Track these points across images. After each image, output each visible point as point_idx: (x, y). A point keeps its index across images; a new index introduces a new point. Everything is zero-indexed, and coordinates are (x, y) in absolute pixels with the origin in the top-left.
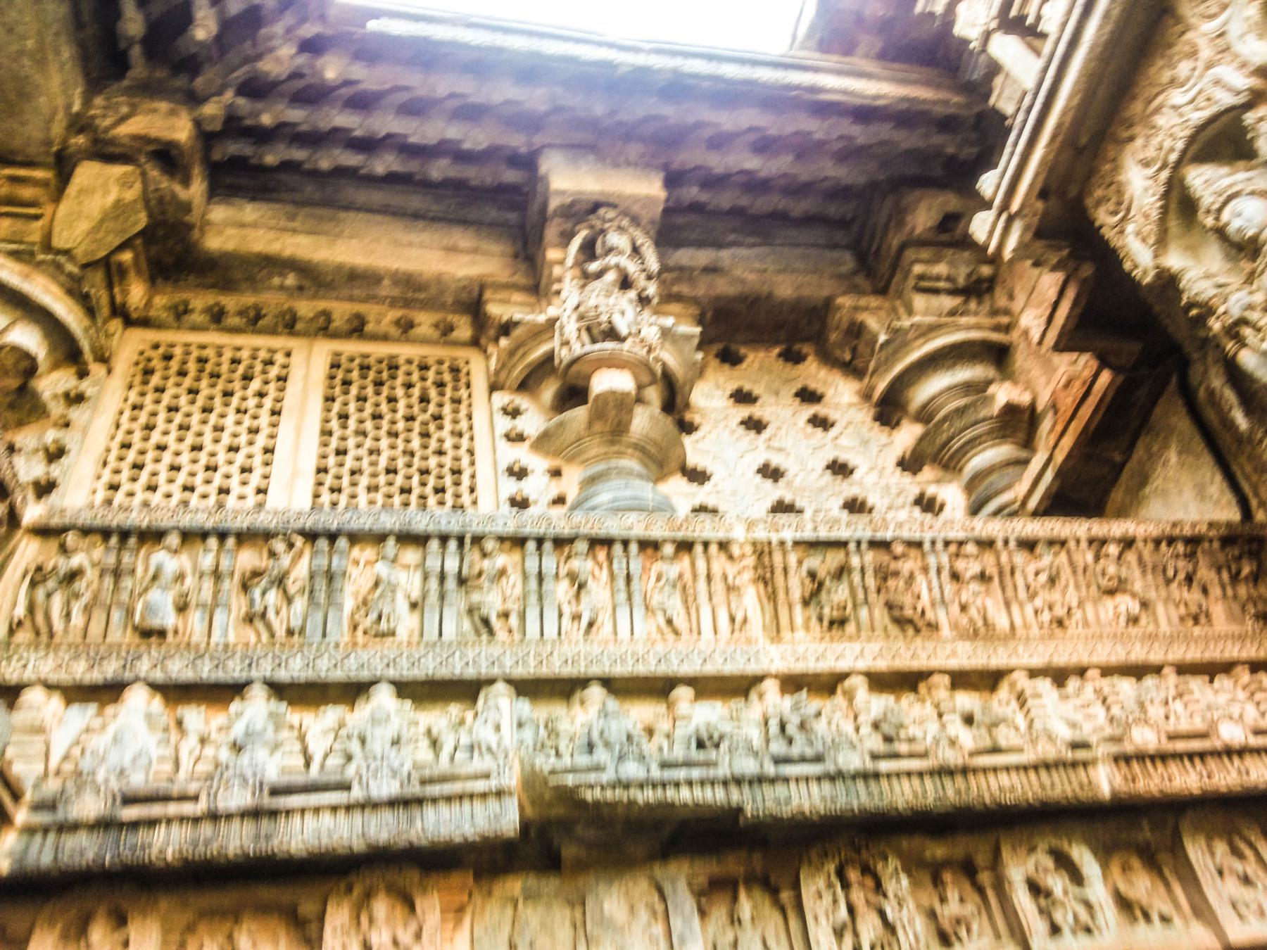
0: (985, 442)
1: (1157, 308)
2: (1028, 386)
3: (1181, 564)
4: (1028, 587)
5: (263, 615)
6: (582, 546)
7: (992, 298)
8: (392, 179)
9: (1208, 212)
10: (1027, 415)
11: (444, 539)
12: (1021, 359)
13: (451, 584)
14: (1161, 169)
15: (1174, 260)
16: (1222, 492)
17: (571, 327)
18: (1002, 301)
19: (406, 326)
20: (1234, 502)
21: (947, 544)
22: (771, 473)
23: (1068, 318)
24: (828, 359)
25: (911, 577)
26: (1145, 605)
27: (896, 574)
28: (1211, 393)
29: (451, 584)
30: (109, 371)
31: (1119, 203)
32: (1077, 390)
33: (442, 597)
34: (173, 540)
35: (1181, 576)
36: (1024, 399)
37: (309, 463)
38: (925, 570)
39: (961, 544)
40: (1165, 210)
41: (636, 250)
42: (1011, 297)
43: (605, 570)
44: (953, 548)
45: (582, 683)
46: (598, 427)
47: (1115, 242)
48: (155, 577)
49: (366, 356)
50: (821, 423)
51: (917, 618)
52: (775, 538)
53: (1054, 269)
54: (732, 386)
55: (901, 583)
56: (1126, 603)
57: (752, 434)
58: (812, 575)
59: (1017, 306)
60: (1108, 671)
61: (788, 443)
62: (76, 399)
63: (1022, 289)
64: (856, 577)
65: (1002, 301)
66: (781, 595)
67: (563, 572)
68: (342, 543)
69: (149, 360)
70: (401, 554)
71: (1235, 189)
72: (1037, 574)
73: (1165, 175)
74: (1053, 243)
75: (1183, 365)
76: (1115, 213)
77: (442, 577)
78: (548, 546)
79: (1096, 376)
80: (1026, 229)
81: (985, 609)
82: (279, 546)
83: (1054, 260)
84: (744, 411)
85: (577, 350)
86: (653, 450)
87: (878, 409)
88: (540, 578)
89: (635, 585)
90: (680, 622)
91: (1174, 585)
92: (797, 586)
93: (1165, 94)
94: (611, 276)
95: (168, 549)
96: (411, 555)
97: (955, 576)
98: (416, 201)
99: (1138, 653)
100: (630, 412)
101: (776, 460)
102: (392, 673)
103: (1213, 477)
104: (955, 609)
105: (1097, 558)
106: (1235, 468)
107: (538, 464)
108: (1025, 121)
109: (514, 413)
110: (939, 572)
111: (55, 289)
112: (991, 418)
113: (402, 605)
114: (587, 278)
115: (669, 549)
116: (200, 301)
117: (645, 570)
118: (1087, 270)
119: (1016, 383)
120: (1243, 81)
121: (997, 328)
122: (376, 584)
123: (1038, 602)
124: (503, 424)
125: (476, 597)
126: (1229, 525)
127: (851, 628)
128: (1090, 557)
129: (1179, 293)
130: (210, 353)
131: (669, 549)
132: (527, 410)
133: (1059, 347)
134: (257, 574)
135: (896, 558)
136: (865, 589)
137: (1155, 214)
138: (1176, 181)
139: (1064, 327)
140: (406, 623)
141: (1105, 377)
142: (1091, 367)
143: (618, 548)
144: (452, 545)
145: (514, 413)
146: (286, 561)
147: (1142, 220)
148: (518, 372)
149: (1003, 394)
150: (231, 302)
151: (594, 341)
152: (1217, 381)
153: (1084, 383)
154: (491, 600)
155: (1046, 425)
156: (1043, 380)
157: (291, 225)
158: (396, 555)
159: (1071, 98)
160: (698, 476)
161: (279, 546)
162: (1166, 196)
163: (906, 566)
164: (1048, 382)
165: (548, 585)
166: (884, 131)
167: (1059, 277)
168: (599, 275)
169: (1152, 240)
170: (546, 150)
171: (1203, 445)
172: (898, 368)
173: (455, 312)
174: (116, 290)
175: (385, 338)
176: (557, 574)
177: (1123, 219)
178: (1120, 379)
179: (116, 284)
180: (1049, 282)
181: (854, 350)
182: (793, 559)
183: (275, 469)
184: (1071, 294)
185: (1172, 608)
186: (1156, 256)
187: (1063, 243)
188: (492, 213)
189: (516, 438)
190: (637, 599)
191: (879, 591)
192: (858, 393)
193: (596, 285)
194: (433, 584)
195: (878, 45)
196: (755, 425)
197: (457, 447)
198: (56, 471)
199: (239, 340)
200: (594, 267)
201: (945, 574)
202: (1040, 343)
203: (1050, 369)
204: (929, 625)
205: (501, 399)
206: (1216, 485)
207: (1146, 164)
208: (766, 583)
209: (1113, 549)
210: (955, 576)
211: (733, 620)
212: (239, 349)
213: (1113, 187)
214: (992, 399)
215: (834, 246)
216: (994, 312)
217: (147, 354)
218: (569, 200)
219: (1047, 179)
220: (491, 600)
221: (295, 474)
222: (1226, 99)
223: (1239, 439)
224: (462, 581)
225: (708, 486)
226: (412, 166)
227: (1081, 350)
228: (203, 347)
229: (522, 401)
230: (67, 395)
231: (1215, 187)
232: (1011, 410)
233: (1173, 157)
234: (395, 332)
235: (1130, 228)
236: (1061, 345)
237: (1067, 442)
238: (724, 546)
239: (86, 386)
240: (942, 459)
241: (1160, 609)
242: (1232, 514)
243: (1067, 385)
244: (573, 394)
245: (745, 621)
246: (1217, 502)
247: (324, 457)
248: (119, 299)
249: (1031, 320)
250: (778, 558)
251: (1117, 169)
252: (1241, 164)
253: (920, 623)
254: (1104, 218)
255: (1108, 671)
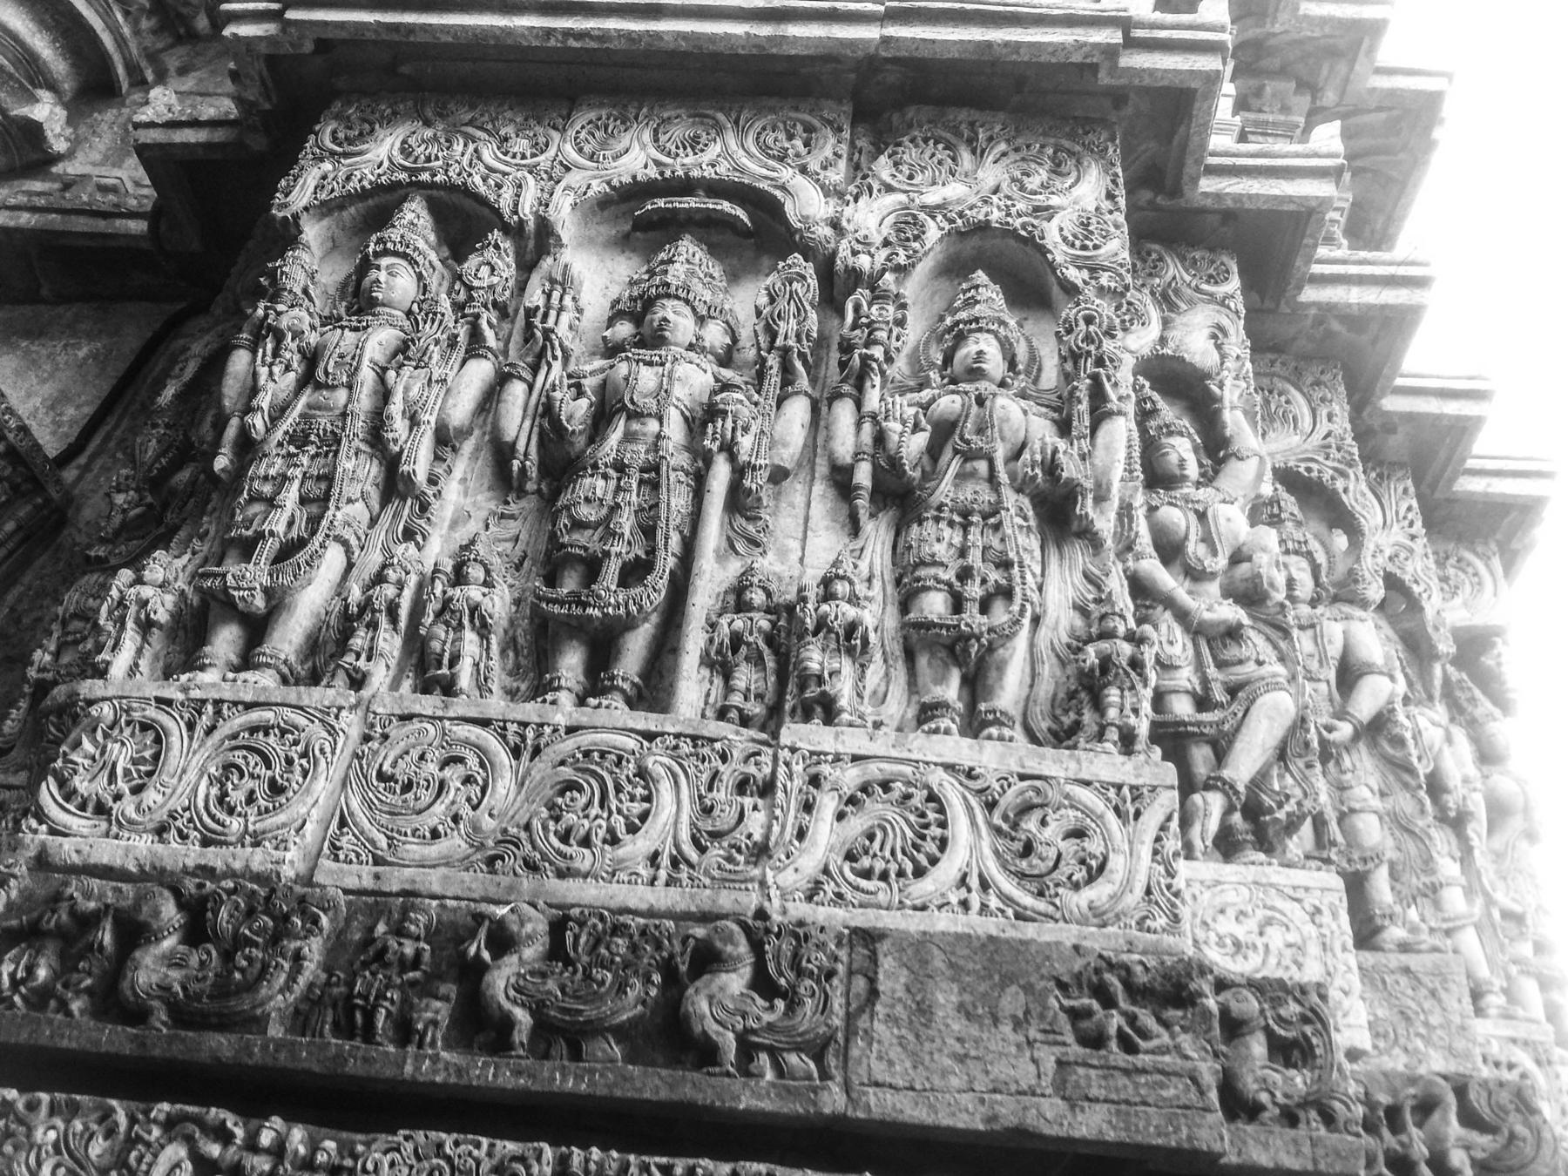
1: (250, 244)
2: (76, 143)
7: (172, 46)
9: (380, 241)
10: (35, 156)
12: (107, 119)
14: (405, 169)
15: (312, 232)
16: (72, 422)
18: (172, 62)
20: (72, 439)
23: (185, 145)
28: (186, 349)
31: (348, 139)
32: (106, 201)
36: (60, 146)
40: (363, 195)
42: (183, 71)
47: (305, 158)
53: (239, 100)
59: (176, 83)
63: (201, 80)
65: (172, 62)
71: (420, 259)
73: (403, 176)
74: (270, 85)
75: (200, 308)
76: (335, 139)
79: (132, 215)
83: (251, 95)
103: (87, 403)
106: (111, 421)
118: (258, 143)
119: (70, 121)
120: (527, 209)
121: (133, 69)
126: (37, 447)
129: (281, 255)
133: (142, 151)
137: (353, 185)
138: (402, 192)
139: (172, 145)
141: (137, 226)
142: (141, 206)
147: (341, 175)
149: (45, 111)
152: (199, 348)
153: (117, 205)
155: (38, 186)
156: (97, 157)
159: (445, 29)
162: (378, 188)
164: (94, 164)
167: (234, 113)
169: (323, 196)
171: (120, 374)
177: (333, 153)
178: (145, 245)
180: (223, 107)
184: (219, 135)
186: (306, 209)
187: (274, 99)
202: (137, 126)
203: (114, 158)
206: (75, 413)
207: (406, 150)
213: (367, 127)
216: (153, 57)
219: (344, 42)
222: (505, 202)
223: (147, 410)
227: (155, 183)
231: (409, 236)
232: (34, 131)
233: (425, 177)
235: (327, 166)
236: (146, 154)
237: (25, 219)
242: (50, 443)
243: (104, 189)
246: (59, 424)
249: (161, 102)
251: (390, 121)
252: (446, 253)
254: (326, 133)
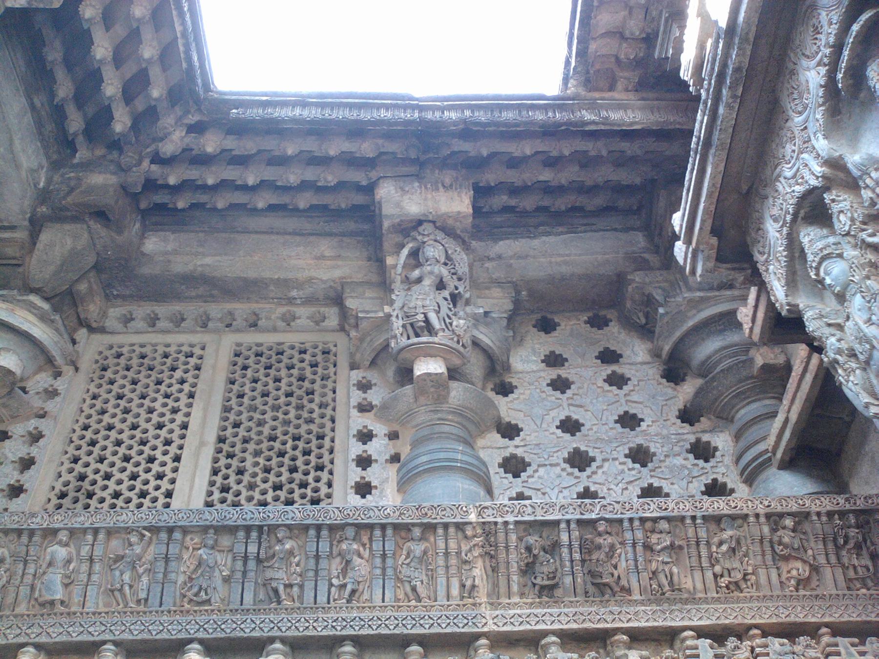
0: (749, 397)
3: (853, 532)
4: (710, 557)
5: (121, 590)
6: (350, 532)
8: (272, 208)
11: (248, 529)
13: (252, 564)
17: (397, 324)
19: (289, 319)
21: (643, 520)
22: (570, 426)
24: (628, 323)
25: (612, 547)
26: (815, 569)
27: (599, 547)
29: (252, 564)
30: (77, 369)
33: (244, 573)
34: (63, 536)
35: (851, 545)
37: (211, 437)
38: (623, 543)
39: (655, 520)
41: (449, 260)
43: (368, 551)
44: (648, 525)
45: (340, 641)
46: (422, 400)
48: (50, 564)
49: (259, 345)
50: (617, 381)
51: (613, 585)
52: (500, 520)
54: (544, 351)
55: (602, 556)
56: (798, 569)
57: (558, 394)
58: (529, 549)
60: (767, 631)
61: (586, 401)
62: (52, 393)
64: (565, 551)
66: (502, 569)
67: (335, 551)
68: (177, 535)
69: (106, 358)
70: (220, 539)
72: (721, 543)
77: (246, 558)
78: (325, 533)
80: (707, 259)
81: (672, 575)
82: (134, 539)
84: (553, 373)
85: (404, 342)
86: (469, 414)
87: (665, 367)
88: (317, 557)
89: (389, 562)
90: (422, 591)
91: (844, 553)
92: (515, 560)
93: (780, 167)
94: (427, 282)
95: (60, 543)
96: (225, 541)
97: (648, 547)
98: (292, 223)
99: (799, 615)
100: (447, 388)
101: (577, 415)
102: (201, 635)
104: (645, 576)
105: (774, 530)
107: (380, 429)
108: (691, 179)
109: (364, 386)
110: (634, 545)
111: (31, 318)
112: (752, 377)
113: (218, 582)
114: (410, 283)
115: (417, 532)
116: (141, 310)
117: (399, 547)
122: (199, 565)
123: (718, 569)
124: (357, 396)
125: (269, 574)
127: (558, 592)
128: (766, 529)
130: (147, 350)
131: (417, 532)
132: (375, 384)
134: (119, 558)
135: (600, 535)
136: (572, 561)
140: (219, 593)
143: (378, 533)
144: (254, 534)
145: (364, 386)
146: (138, 549)
148: (368, 357)
150: (162, 310)
151: (417, 335)
154: (279, 575)
157: (201, 250)
158: (216, 541)
160: (510, 431)
161: (134, 539)
163: (606, 541)
165: (323, 564)
166: (651, 144)
168: (419, 280)
170: (381, 181)
172: (678, 334)
173: (326, 305)
174: (80, 309)
175: (275, 330)
176: (331, 552)
179: (80, 305)
181: (647, 316)
182: (513, 537)
183: (187, 442)
185: (839, 571)
188: (351, 225)
189: (364, 408)
190: (389, 572)
191: (583, 561)
192: (650, 351)
193: (416, 288)
194: (239, 564)
195: (634, 76)
196: (561, 385)
197: (322, 416)
198: (34, 451)
199: (169, 338)
200: (416, 273)
201: (639, 548)
204: (623, 589)
205: (356, 375)
208: (492, 557)
209: (789, 522)
210: (648, 547)
211: (463, 586)
212: (168, 346)
214: (751, 360)
215: (627, 230)
217: (108, 353)
218: (398, 220)
220: (279, 575)
221: (202, 444)
224: (259, 561)
225: (517, 441)
226: (285, 199)
228: (142, 346)
229: (372, 376)
230: (46, 391)
234: (281, 324)
238: (460, 527)
239: (60, 384)
240: (715, 410)
241: (828, 572)
244: (405, 374)
245: (474, 586)
247: (225, 429)
248: (82, 316)
250: (501, 536)
253: (617, 589)
255: (767, 631)
